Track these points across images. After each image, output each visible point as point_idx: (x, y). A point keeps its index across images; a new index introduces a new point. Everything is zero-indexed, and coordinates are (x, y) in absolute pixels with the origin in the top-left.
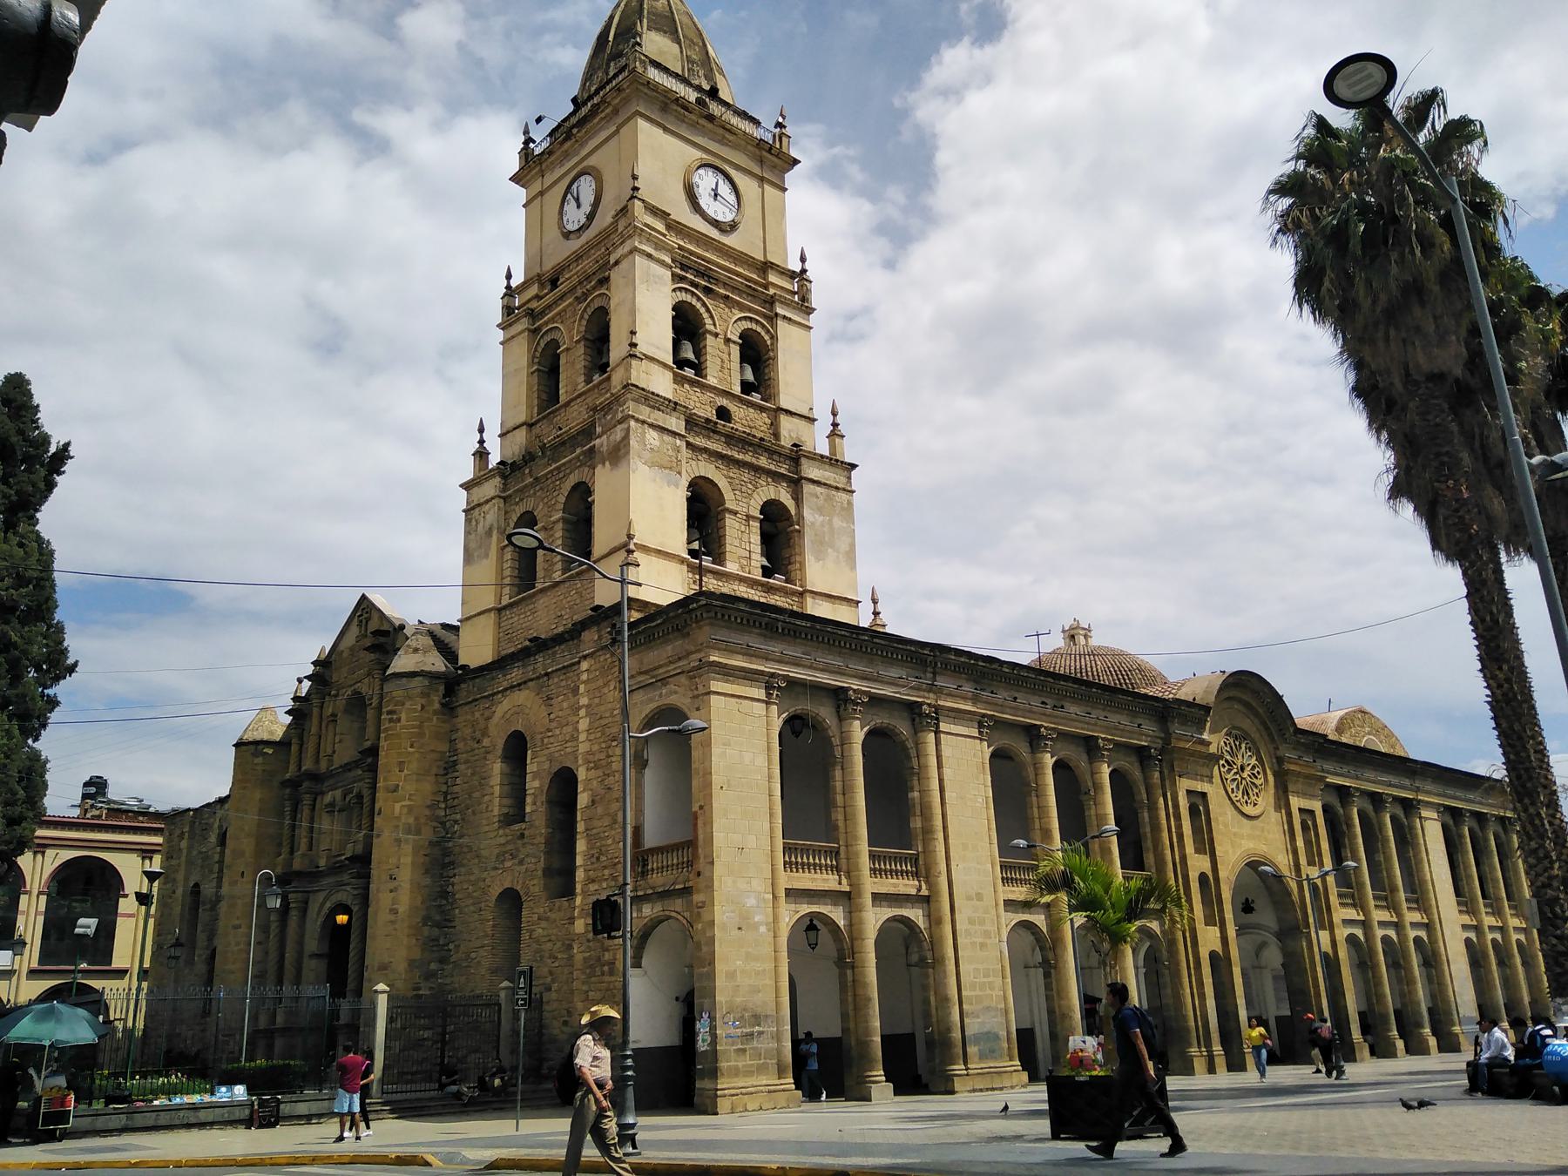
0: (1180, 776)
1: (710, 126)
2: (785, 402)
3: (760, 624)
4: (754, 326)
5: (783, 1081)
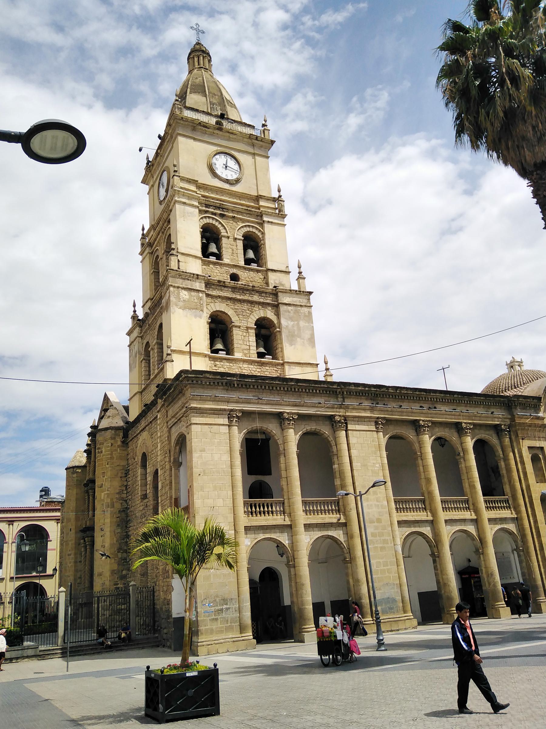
0: (523, 439)
1: (220, 133)
2: (270, 265)
3: (222, 383)
4: (251, 229)
5: (243, 635)
